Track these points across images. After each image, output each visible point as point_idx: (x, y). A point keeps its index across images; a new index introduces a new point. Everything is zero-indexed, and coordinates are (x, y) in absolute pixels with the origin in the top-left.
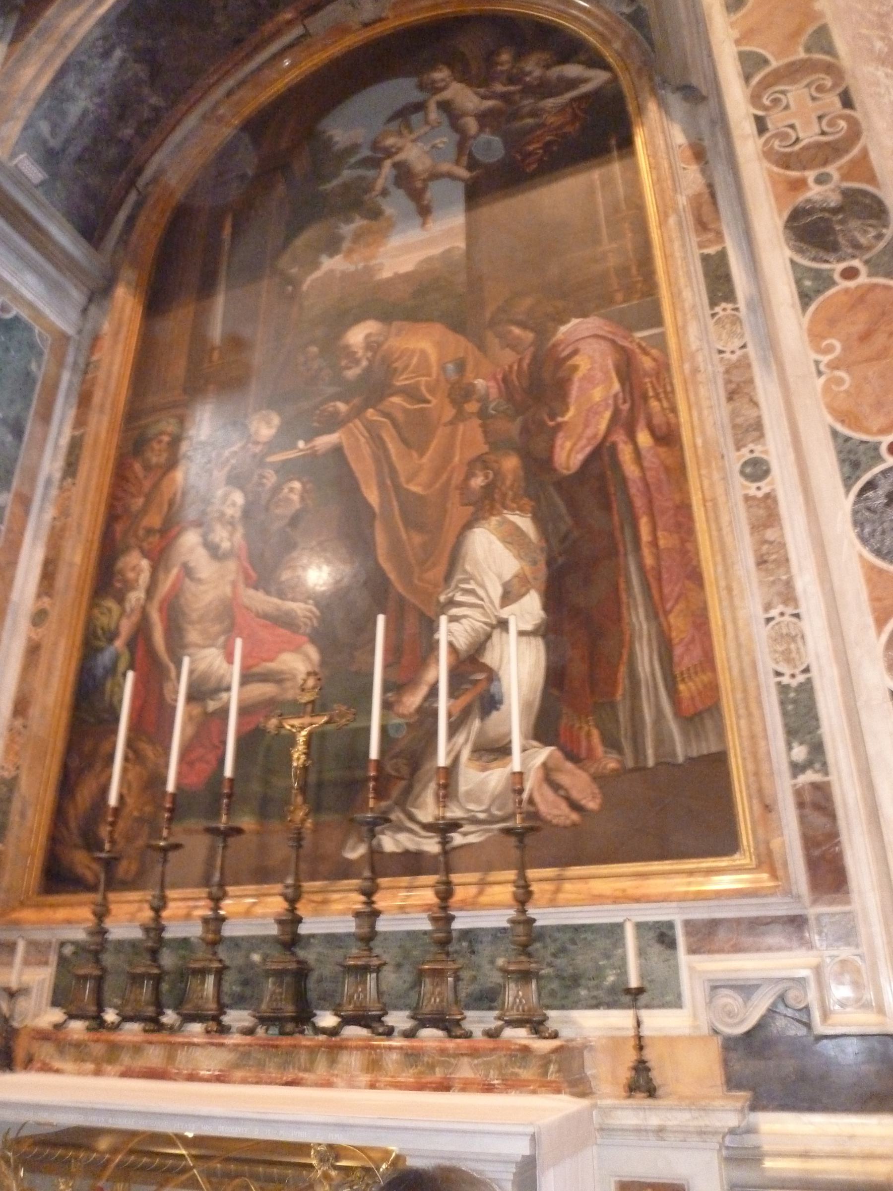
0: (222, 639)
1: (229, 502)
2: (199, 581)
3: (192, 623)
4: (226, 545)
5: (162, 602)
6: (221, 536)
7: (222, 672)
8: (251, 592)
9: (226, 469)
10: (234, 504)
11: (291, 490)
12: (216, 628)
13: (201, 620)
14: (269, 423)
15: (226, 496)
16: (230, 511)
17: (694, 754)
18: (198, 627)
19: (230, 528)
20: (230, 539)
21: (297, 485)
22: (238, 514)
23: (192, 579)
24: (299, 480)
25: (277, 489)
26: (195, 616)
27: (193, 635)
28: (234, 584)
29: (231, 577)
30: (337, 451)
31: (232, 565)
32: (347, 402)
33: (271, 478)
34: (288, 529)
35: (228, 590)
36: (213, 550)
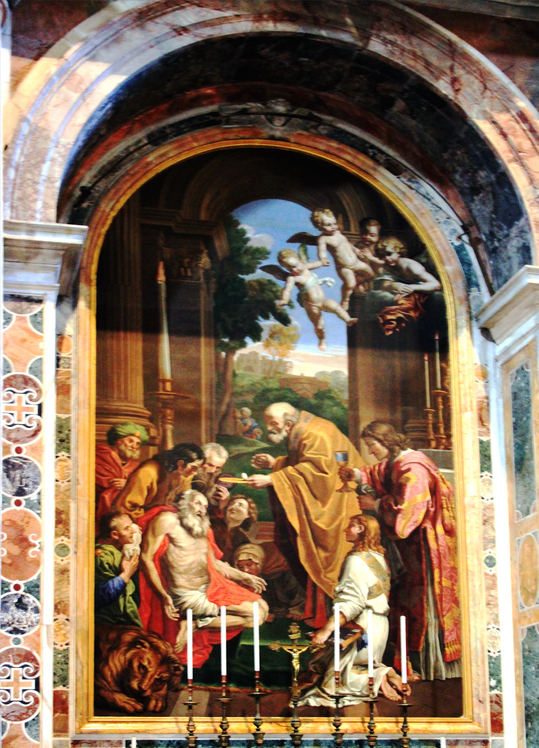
0: (203, 586)
1: (196, 501)
2: (180, 547)
3: (180, 573)
4: (197, 529)
5: (155, 555)
6: (192, 521)
7: (205, 606)
8: (220, 562)
9: (191, 477)
10: (200, 503)
11: (241, 504)
12: (198, 580)
13: (186, 572)
14: (219, 454)
15: (192, 497)
16: (197, 508)
17: (450, 677)
18: (184, 576)
19: (199, 518)
20: (201, 525)
21: (244, 502)
22: (204, 511)
23: (175, 545)
24: (246, 499)
25: (231, 501)
26: (181, 569)
27: (180, 580)
28: (207, 555)
29: (205, 550)
30: (270, 488)
31: (203, 544)
32: (275, 456)
33: (225, 494)
34: (241, 530)
35: (204, 558)
36: (189, 530)
